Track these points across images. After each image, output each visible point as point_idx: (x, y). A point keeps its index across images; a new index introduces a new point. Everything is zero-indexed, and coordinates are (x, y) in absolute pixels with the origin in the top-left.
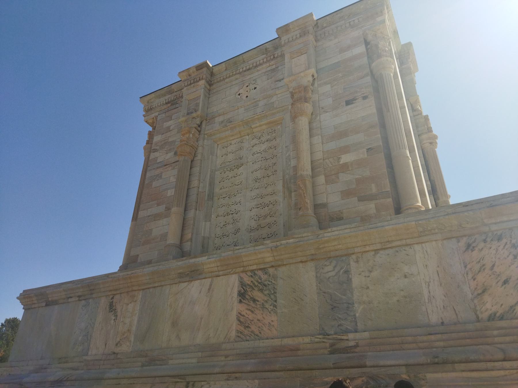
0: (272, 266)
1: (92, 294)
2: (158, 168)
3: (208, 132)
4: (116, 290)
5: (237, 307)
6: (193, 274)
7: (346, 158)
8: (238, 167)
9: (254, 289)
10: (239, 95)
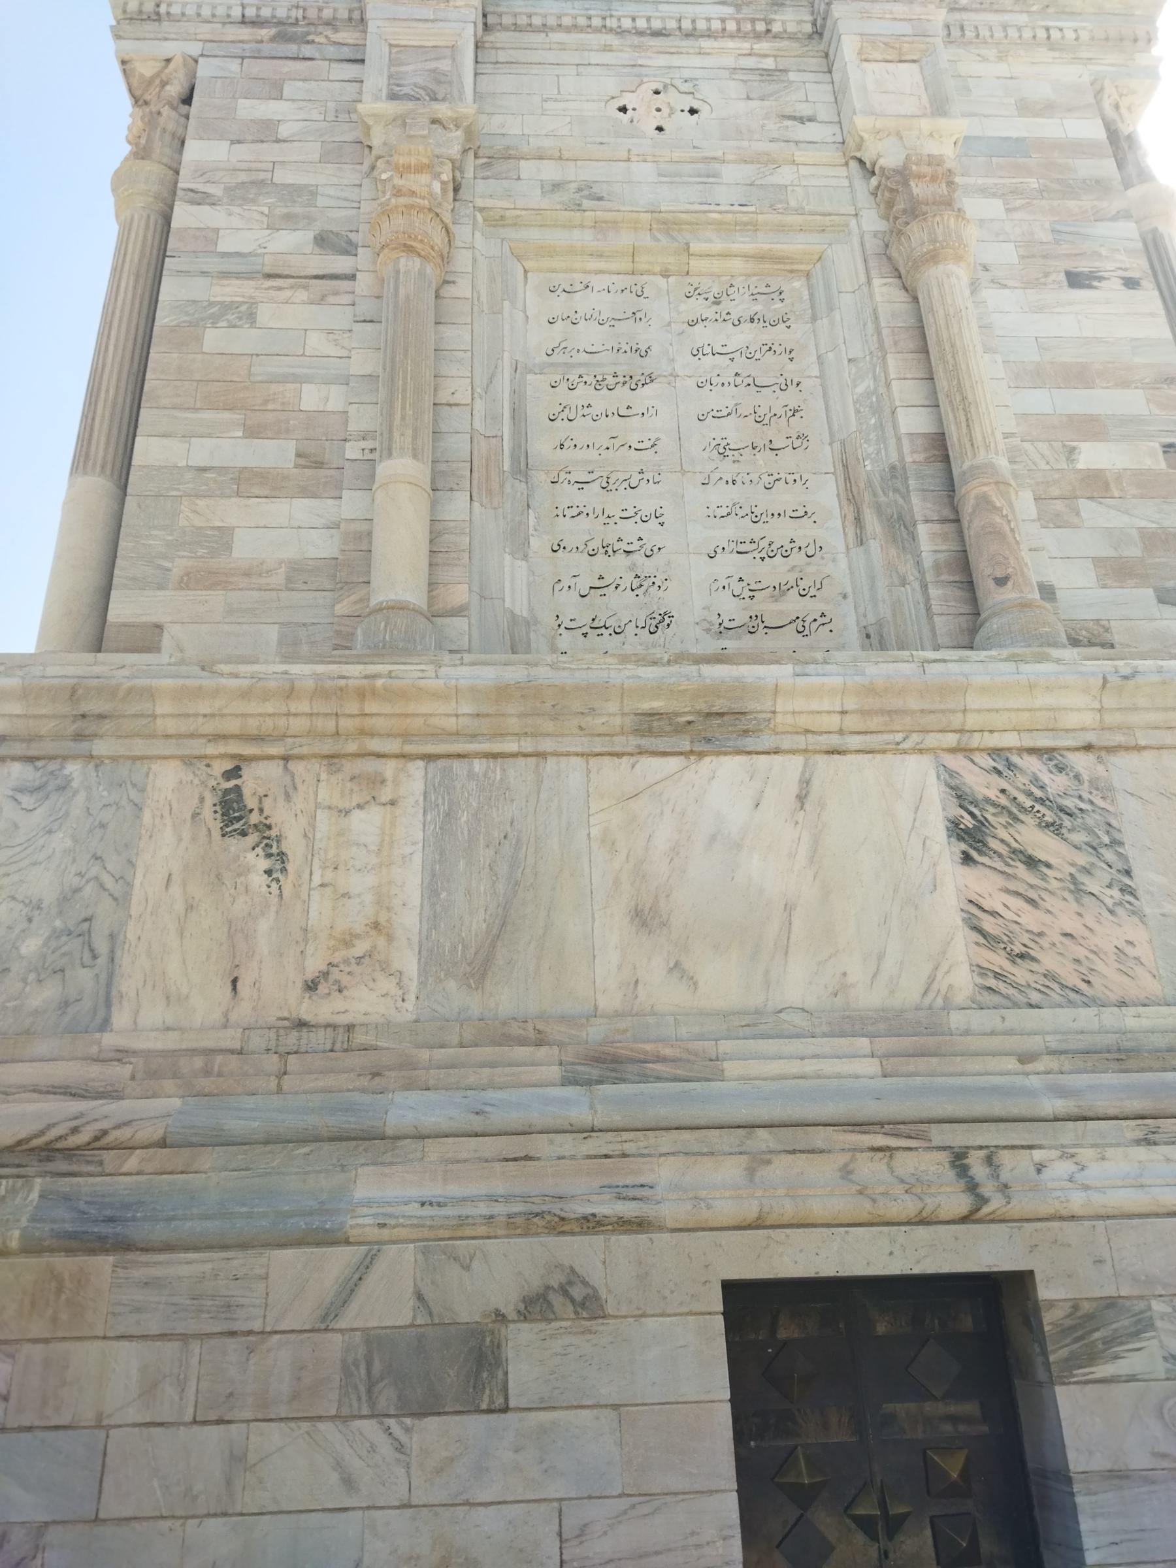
0: (1088, 748)
1: (79, 737)
2: (225, 275)
3: (489, 203)
4: (258, 739)
5: (955, 881)
7: (1094, 456)
8: (635, 383)
9: (1016, 819)
10: (623, 109)
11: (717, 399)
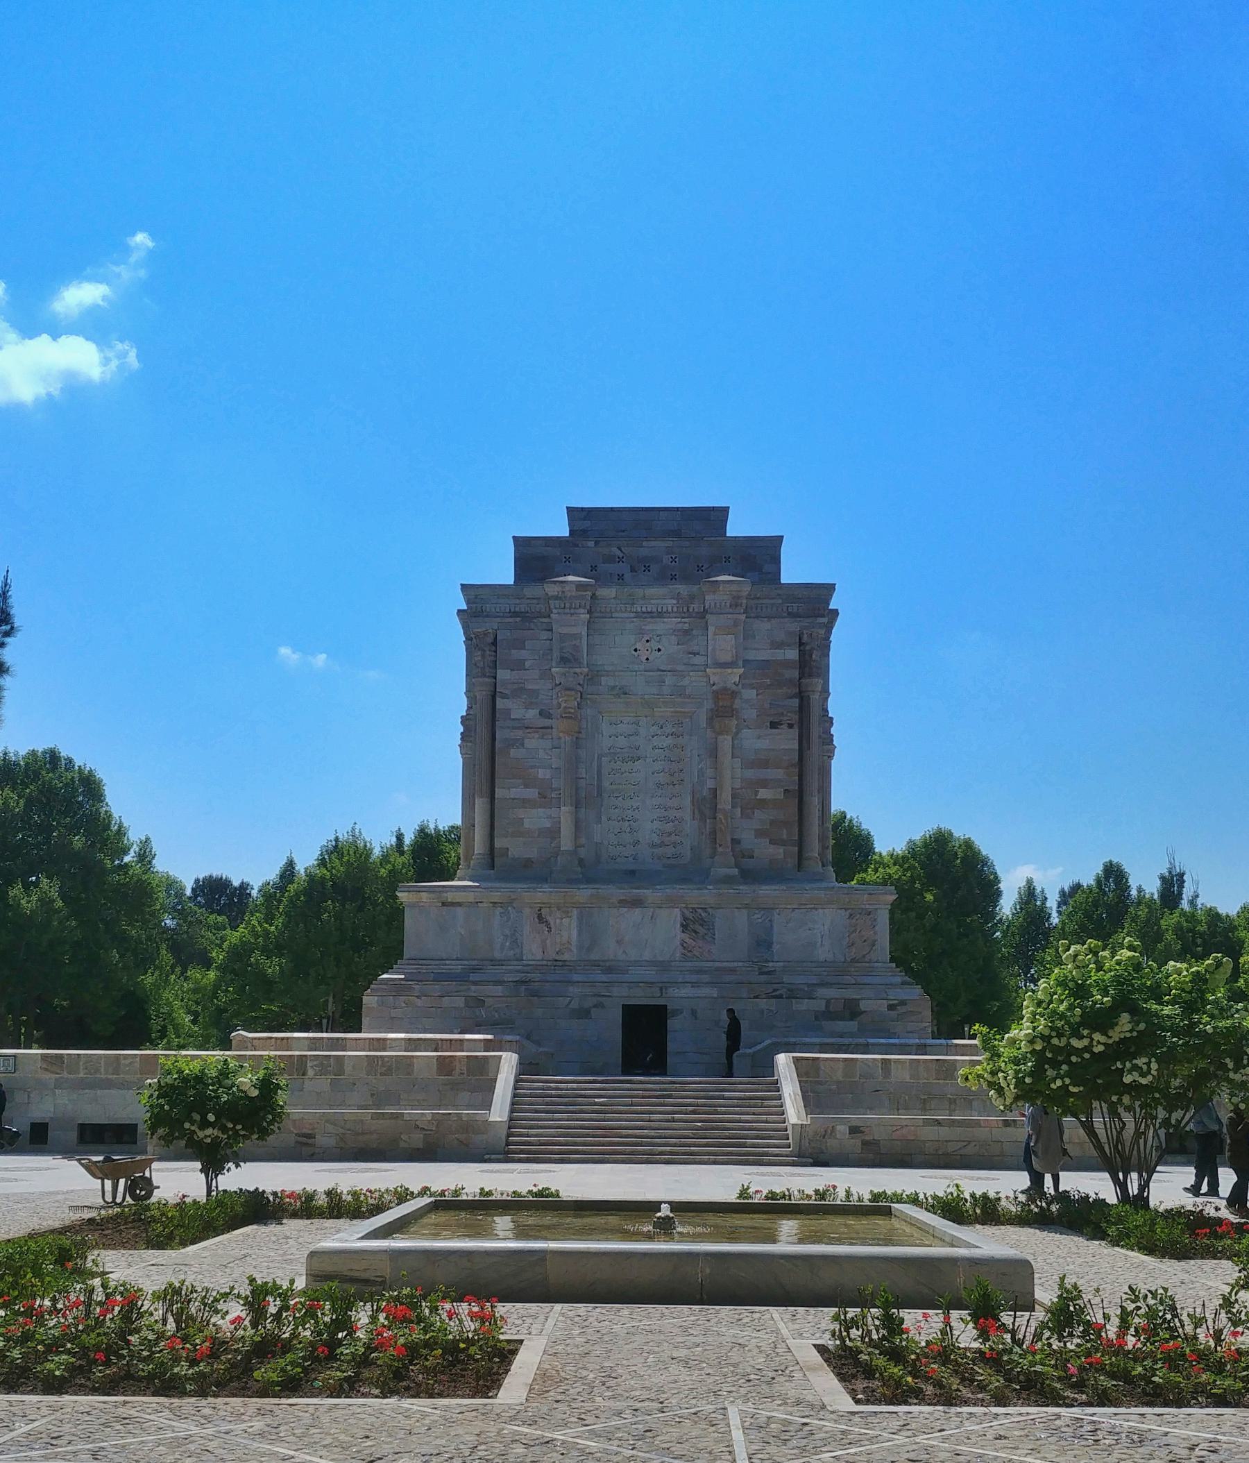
2: (514, 728)
5: (680, 936)
6: (637, 903)
7: (764, 794)
11: (658, 766)
